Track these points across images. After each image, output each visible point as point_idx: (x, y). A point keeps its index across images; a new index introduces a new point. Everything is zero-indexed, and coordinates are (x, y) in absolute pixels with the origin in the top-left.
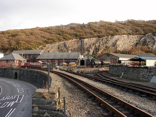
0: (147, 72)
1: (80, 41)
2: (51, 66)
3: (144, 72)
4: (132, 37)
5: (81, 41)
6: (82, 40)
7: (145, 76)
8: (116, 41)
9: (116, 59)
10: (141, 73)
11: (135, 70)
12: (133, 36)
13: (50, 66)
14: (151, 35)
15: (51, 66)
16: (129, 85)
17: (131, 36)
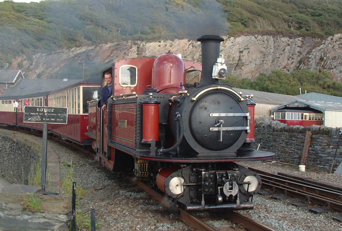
0: (329, 145)
1: (135, 48)
2: (53, 117)
3: (320, 145)
4: (288, 42)
5: (138, 48)
7: (321, 157)
8: (241, 52)
11: (294, 139)
12: (291, 40)
13: (49, 117)
15: (53, 117)
16: (276, 180)
17: (285, 39)
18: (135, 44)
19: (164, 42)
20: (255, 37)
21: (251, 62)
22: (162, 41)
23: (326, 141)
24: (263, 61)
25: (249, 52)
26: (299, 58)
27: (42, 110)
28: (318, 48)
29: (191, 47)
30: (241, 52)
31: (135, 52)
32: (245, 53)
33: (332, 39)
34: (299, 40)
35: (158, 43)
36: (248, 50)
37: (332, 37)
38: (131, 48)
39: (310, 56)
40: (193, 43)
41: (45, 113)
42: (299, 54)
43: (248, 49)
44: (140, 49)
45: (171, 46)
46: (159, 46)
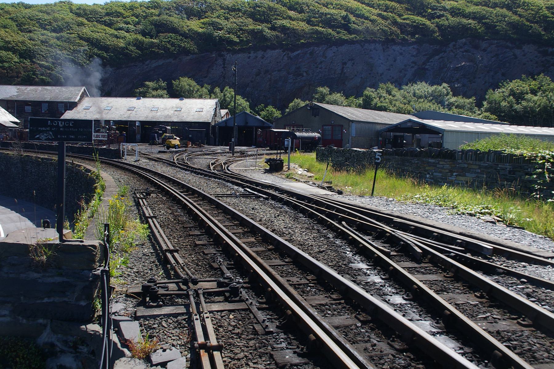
0: (451, 172)
1: (220, 61)
3: (440, 172)
6: (228, 57)
9: (342, 126)
10: (428, 176)
12: (403, 48)
14: (465, 44)
18: (221, 56)
19: (254, 53)
20: (361, 46)
21: (356, 76)
22: (252, 52)
23: (447, 166)
24: (370, 74)
25: (353, 64)
26: (413, 69)
27: (55, 123)
28: (437, 57)
29: (286, 58)
30: (345, 64)
31: (221, 65)
32: (349, 64)
33: (454, 45)
34: (414, 48)
35: (246, 55)
36: (353, 62)
37: (454, 43)
38: (216, 60)
39: (427, 67)
40: (288, 54)
41: (61, 127)
42: (413, 65)
43: (352, 60)
44: (226, 61)
45: (263, 58)
46: (249, 57)
